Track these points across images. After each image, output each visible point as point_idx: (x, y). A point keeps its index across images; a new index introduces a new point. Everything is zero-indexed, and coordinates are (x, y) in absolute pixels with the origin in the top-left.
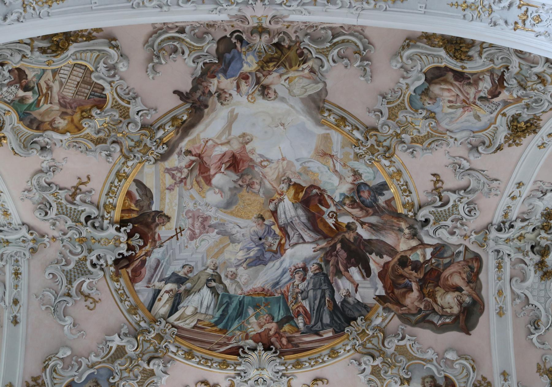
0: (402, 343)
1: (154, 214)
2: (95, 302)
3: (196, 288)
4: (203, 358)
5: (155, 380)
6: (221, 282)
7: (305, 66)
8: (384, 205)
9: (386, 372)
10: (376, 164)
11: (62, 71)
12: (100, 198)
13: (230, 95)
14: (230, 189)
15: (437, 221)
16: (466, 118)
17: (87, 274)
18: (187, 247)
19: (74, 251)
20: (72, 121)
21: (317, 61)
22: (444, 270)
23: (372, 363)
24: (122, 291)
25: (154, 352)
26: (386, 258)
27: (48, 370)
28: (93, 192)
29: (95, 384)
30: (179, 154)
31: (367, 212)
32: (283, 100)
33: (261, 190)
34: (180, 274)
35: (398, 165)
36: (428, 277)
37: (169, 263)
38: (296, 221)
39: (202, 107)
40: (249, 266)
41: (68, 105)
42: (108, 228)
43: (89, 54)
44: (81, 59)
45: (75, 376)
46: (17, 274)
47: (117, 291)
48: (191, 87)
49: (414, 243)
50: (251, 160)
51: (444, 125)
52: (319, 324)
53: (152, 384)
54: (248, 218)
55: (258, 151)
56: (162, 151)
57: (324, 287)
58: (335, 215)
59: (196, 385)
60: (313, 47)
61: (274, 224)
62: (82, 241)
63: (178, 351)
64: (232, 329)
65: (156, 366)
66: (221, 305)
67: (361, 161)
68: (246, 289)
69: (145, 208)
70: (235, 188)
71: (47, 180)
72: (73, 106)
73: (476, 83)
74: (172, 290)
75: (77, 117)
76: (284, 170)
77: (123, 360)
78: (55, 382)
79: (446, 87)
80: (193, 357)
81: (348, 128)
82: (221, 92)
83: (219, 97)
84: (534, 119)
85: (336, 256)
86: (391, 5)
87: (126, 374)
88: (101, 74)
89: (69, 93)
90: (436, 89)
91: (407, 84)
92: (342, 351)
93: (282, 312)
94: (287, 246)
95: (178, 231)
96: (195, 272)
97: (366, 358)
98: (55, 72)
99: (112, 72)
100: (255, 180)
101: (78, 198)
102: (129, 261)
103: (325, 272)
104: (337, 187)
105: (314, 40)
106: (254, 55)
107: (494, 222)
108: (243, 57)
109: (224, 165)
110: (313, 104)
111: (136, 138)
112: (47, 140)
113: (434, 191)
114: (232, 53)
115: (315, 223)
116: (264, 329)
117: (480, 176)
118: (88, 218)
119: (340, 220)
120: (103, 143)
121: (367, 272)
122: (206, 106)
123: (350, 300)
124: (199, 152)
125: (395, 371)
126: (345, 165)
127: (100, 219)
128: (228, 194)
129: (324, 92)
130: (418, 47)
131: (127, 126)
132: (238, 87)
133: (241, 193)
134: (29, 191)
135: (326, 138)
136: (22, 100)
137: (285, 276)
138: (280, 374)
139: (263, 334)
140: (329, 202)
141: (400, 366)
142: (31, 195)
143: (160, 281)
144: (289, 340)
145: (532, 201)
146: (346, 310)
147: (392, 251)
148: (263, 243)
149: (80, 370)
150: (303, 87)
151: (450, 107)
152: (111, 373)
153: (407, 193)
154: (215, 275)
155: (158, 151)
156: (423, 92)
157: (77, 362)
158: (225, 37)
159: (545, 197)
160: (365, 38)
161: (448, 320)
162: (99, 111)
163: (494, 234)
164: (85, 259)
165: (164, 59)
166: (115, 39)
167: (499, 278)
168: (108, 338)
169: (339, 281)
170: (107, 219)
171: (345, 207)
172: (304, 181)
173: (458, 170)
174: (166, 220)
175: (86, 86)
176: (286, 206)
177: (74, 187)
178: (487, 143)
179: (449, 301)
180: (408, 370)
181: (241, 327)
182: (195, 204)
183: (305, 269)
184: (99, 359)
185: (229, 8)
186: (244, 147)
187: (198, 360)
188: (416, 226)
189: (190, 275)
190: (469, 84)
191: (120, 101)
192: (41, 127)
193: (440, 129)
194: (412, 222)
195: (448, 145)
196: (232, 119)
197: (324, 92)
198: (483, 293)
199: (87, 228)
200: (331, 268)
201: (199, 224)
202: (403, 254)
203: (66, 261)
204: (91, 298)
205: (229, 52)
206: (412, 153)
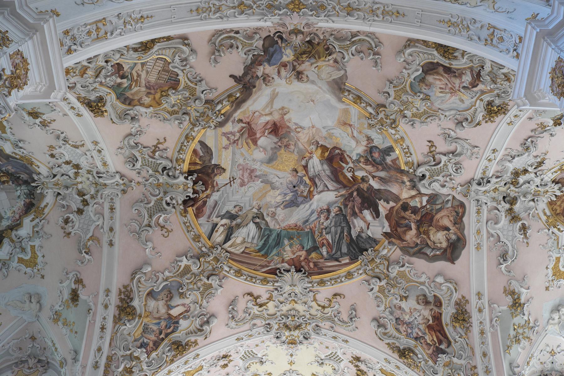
0: (402, 269)
1: (213, 166)
2: (168, 231)
3: (245, 223)
5: (213, 291)
6: (264, 219)
7: (330, 57)
8: (391, 163)
9: (389, 291)
10: (384, 132)
11: (148, 64)
12: (173, 154)
13: (273, 78)
14: (272, 149)
15: (431, 176)
16: (452, 101)
19: (153, 193)
20: (154, 98)
21: (339, 54)
22: (436, 214)
23: (379, 283)
24: (189, 224)
26: (392, 204)
27: (135, 281)
28: (168, 150)
29: (168, 292)
30: (233, 122)
31: (377, 168)
32: (313, 82)
33: (296, 150)
34: (232, 212)
35: (402, 133)
36: (423, 219)
37: (224, 204)
39: (251, 88)
40: (286, 207)
41: (152, 88)
42: (179, 177)
43: (168, 51)
44: (162, 54)
46: (112, 209)
48: (243, 72)
49: (413, 193)
50: (288, 127)
51: (437, 105)
52: (339, 253)
54: (285, 171)
55: (294, 121)
56: (219, 120)
57: (343, 225)
58: (352, 170)
60: (336, 44)
61: (305, 176)
62: (159, 186)
64: (272, 255)
65: (214, 281)
66: (263, 236)
67: (373, 129)
68: (283, 225)
69: (206, 162)
70: (275, 147)
71: (135, 141)
72: (155, 88)
73: (460, 76)
74: (226, 224)
75: (158, 96)
76: (313, 135)
77: (189, 276)
79: (438, 77)
80: (242, 275)
81: (363, 105)
82: (265, 76)
83: (264, 80)
84: (503, 104)
86: (395, 18)
88: (176, 65)
89: (153, 79)
90: (430, 78)
91: (408, 73)
92: (356, 274)
93: (310, 243)
94: (315, 193)
95: (232, 179)
97: (374, 280)
98: (143, 64)
99: (185, 63)
100: (291, 142)
101: (157, 154)
103: (344, 213)
104: (354, 148)
105: (337, 39)
106: (291, 49)
107: (475, 178)
108: (283, 51)
109: (267, 131)
110: (336, 86)
111: (201, 109)
112: (135, 112)
113: (429, 154)
114: (274, 48)
115: (336, 175)
117: (465, 144)
118: (164, 169)
119: (356, 174)
120: (176, 114)
121: (377, 214)
122: (254, 87)
123: (363, 235)
124: (248, 120)
125: (396, 290)
126: (360, 132)
127: (173, 170)
128: (270, 152)
129: (344, 77)
130: (417, 47)
131: (195, 102)
132: (279, 72)
133: (280, 152)
134: (121, 148)
135: (346, 112)
136: (120, 85)
137: (313, 215)
138: (308, 290)
139: (295, 260)
140: (348, 159)
141: (400, 287)
142: (123, 151)
143: (217, 217)
144: (316, 264)
145: (504, 163)
147: (397, 199)
148: (296, 190)
150: (328, 73)
151: (441, 92)
152: (181, 286)
153: (409, 155)
155: (218, 120)
156: (420, 80)
157: (155, 275)
158: (270, 36)
159: (514, 160)
160: (376, 38)
161: (438, 253)
162: (174, 92)
163: (475, 187)
164: (161, 199)
165: (224, 52)
166: (187, 39)
167: (478, 221)
168: (178, 259)
169: (355, 221)
170: (178, 170)
172: (329, 144)
173: (447, 138)
174: (222, 171)
175: (165, 73)
176: (315, 162)
177: (154, 146)
178: (470, 120)
179: (439, 238)
182: (244, 159)
183: (328, 211)
184: (171, 275)
185: (272, 18)
186: (283, 117)
187: (245, 277)
188: (415, 180)
189: (240, 213)
190: (455, 76)
191: (189, 83)
192: (132, 103)
193: (434, 108)
194: (412, 176)
195: (440, 119)
196: (274, 96)
197: (344, 77)
198: (466, 232)
200: (349, 211)
201: (248, 175)
202: (404, 201)
203: (147, 200)
205: (273, 47)
206: (413, 125)
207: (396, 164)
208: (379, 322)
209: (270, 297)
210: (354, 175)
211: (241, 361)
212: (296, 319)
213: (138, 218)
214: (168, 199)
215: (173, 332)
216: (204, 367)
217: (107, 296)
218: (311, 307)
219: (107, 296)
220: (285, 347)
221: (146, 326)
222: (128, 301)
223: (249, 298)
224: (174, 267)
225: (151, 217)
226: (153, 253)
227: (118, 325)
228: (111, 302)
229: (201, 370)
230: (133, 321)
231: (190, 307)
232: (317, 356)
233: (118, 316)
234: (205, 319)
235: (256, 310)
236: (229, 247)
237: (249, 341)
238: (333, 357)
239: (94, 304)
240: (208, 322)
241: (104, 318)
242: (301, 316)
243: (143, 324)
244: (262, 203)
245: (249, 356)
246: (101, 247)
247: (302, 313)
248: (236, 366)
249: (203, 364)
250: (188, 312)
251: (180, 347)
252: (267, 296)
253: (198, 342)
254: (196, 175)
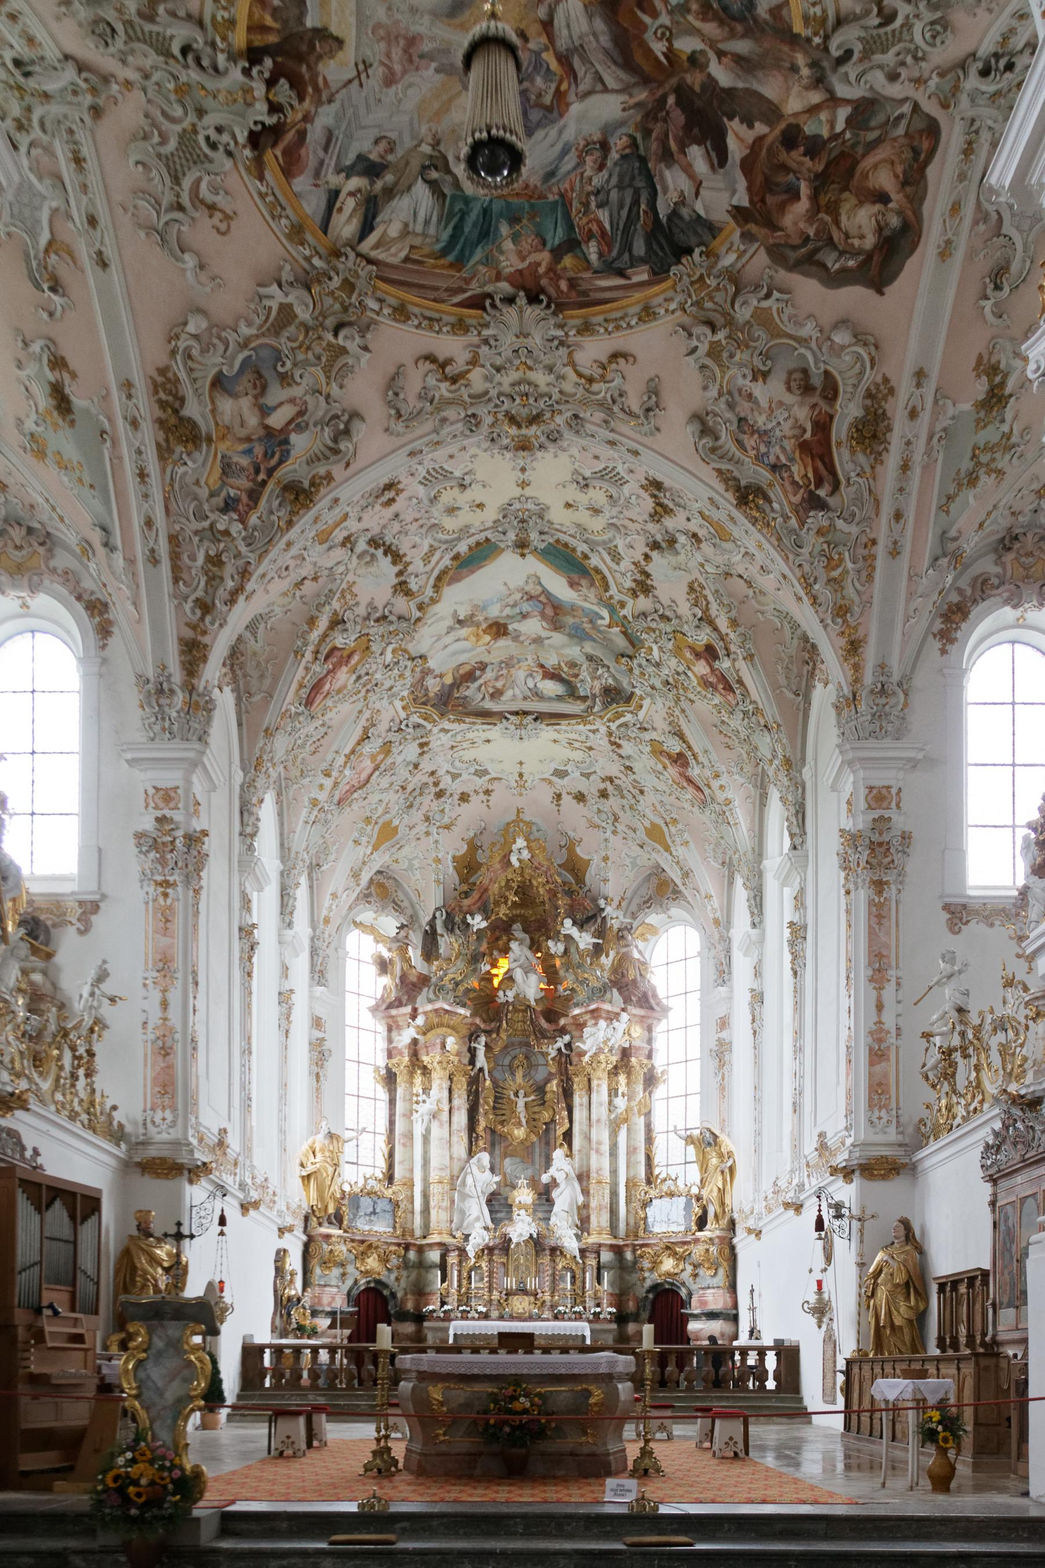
0: (765, 304)
4: (425, 318)
5: (350, 361)
6: (448, 171)
22: (864, 156)
26: (760, 128)
38: (591, 44)
49: (816, 97)
52: (626, 256)
57: (640, 183)
58: (668, 35)
61: (547, 49)
64: (472, 263)
66: (451, 215)
77: (292, 329)
85: (665, 121)
87: (301, 357)
92: (662, 311)
93: (560, 230)
94: (572, 97)
95: (361, 67)
103: (642, 152)
118: (185, 50)
119: (678, 44)
146: (676, 230)
168: (263, 291)
169: (667, 174)
171: (690, 18)
174: (335, 45)
179: (861, 222)
180: (766, 356)
183: (604, 146)
184: (253, 331)
194: (817, 55)
200: (654, 146)
202: (792, 120)
207: (781, 18)
208: (703, 424)
210: (670, 49)
212: (531, 401)
218: (563, 378)
220: (508, 455)
225: (177, 180)
226: (203, 278)
232: (576, 472)
234: (342, 426)
238: (608, 475)
240: (347, 432)
242: (542, 396)
245: (437, 476)
247: (543, 388)
252: (467, 356)
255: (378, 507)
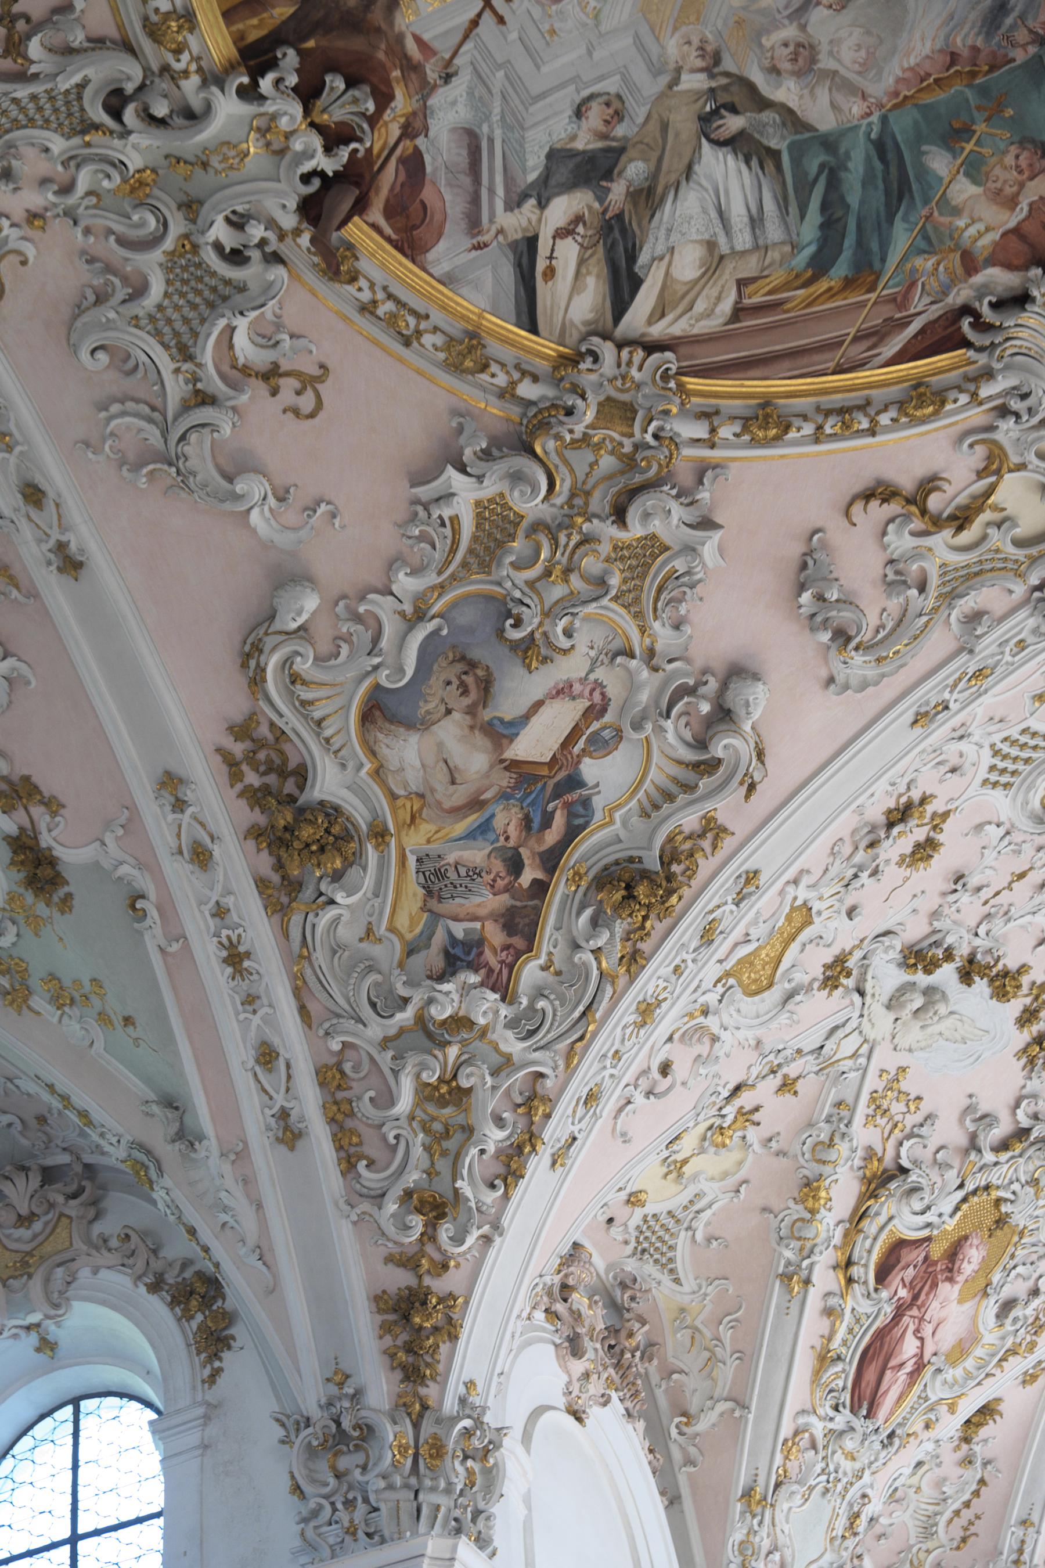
2: (308, 382)
3: (672, 165)
17: (225, 299)
18: (553, 32)
25: (622, 473)
29: (460, 667)
34: (579, 145)
37: (514, 125)
42: (208, 108)
45: (376, 668)
47: (368, 309)
53: (670, 585)
59: (847, 514)
62: (138, 189)
63: (713, 431)
68: (881, 86)
77: (517, 545)
78: (317, 715)
80: (787, 428)
87: (557, 592)
96: (639, 112)
101: (34, 48)
102: (357, 184)
116: (1024, 206)
118: (116, 102)
127: (165, 85)
139: (1029, 228)
143: (514, 203)
149: (384, 643)
152: (504, 611)
154: (725, 88)
157: (358, 618)
164: (189, 245)
168: (424, 492)
170: (186, 73)
181: (927, 238)
184: (432, 579)
187: (808, 429)
189: (620, 131)
199: (133, 138)
203: (125, 280)
204: (287, 374)
209: (990, 458)
211: (999, 792)
213: (129, 385)
214: (219, 231)
215: (572, 833)
216: (816, 906)
217: (180, 805)
219: (180, 805)
221: (429, 866)
222: (290, 787)
223: (878, 511)
224: (423, 537)
225: (185, 353)
226: (292, 517)
227: (296, 919)
228: (212, 828)
229: (808, 922)
230: (354, 872)
231: (598, 684)
233: (276, 878)
234: (705, 708)
235: (943, 550)
236: (650, 322)
237: (987, 699)
239: (140, 866)
241: (220, 912)
243: (412, 861)
244: (712, 27)
246: (33, 594)
248: (979, 827)
249: (802, 894)
250: (604, 710)
251: (641, 891)
253: (722, 818)
254: (290, 58)
255: (892, 874)
